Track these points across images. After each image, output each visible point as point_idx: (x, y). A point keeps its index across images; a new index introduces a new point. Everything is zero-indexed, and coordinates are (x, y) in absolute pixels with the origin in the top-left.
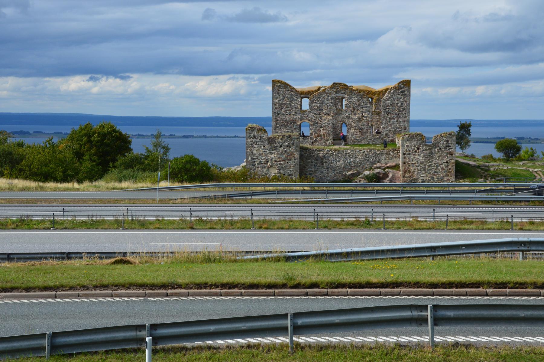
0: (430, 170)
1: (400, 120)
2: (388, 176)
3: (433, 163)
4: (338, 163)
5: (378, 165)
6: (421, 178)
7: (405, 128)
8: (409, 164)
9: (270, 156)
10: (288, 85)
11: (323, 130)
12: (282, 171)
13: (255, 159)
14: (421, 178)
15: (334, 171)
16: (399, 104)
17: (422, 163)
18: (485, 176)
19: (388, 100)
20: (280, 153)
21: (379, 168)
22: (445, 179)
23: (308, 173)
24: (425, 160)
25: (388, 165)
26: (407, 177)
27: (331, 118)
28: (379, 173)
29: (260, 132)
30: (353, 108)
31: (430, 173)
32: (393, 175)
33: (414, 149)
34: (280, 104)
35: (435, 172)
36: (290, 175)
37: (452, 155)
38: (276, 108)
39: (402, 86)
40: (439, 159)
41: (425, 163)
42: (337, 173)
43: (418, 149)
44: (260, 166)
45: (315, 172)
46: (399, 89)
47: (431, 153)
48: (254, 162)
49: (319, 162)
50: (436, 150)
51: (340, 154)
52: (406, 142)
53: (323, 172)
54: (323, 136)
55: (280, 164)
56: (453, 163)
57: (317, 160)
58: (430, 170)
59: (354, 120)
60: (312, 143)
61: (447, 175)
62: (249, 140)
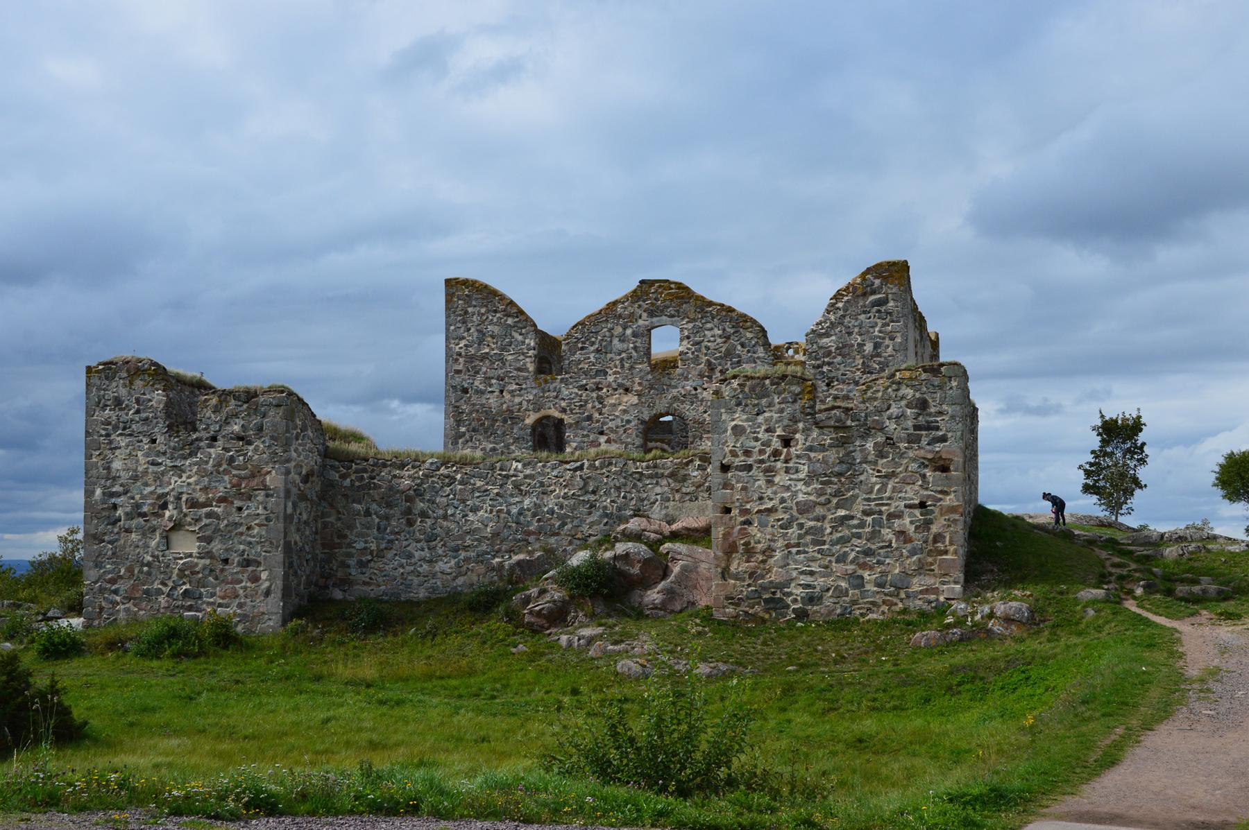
0: (843, 541)
2: (665, 573)
3: (859, 507)
4: (471, 517)
5: (634, 524)
6: (804, 579)
8: (745, 512)
9: (175, 483)
10: (494, 293)
11: (608, 441)
12: (217, 547)
13: (117, 495)
14: (804, 579)
15: (456, 550)
16: (869, 347)
17: (804, 508)
18: (1121, 578)
19: (827, 335)
20: (209, 467)
21: (637, 537)
22: (916, 584)
23: (352, 562)
24: (820, 493)
25: (674, 527)
26: (736, 577)
27: (635, 400)
28: (626, 557)
29: (138, 383)
30: (709, 363)
31: (842, 559)
32: (684, 569)
33: (767, 444)
34: (470, 359)
35: (868, 553)
36: (247, 563)
38: (458, 372)
39: (877, 282)
40: (884, 486)
41: (819, 511)
42: (467, 560)
43: (787, 442)
44: (134, 523)
45: (380, 554)
46: (865, 295)
47: (848, 461)
48: (115, 507)
49: (396, 511)
50: (870, 445)
51: (480, 477)
52: (731, 411)
53: (410, 556)
55: (209, 515)
56: (952, 509)
57: (389, 505)
58: (843, 541)
61: (922, 569)
62: (100, 416)
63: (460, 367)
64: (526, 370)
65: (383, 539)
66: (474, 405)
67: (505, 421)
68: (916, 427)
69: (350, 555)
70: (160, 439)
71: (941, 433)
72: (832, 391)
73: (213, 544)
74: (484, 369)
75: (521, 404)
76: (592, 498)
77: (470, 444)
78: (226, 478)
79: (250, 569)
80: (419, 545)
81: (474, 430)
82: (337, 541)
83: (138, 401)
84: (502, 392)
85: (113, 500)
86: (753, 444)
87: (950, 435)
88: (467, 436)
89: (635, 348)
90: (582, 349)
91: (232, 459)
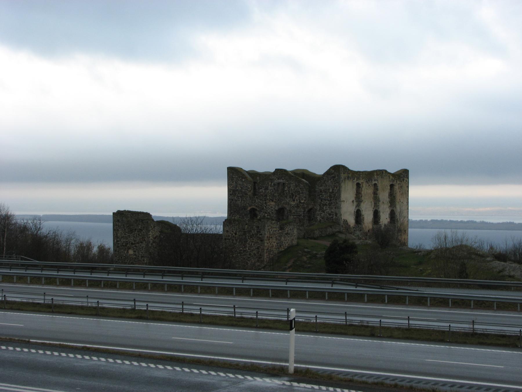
7: (336, 215)
16: (331, 190)
36: (142, 257)
37: (262, 241)
91: (139, 234)
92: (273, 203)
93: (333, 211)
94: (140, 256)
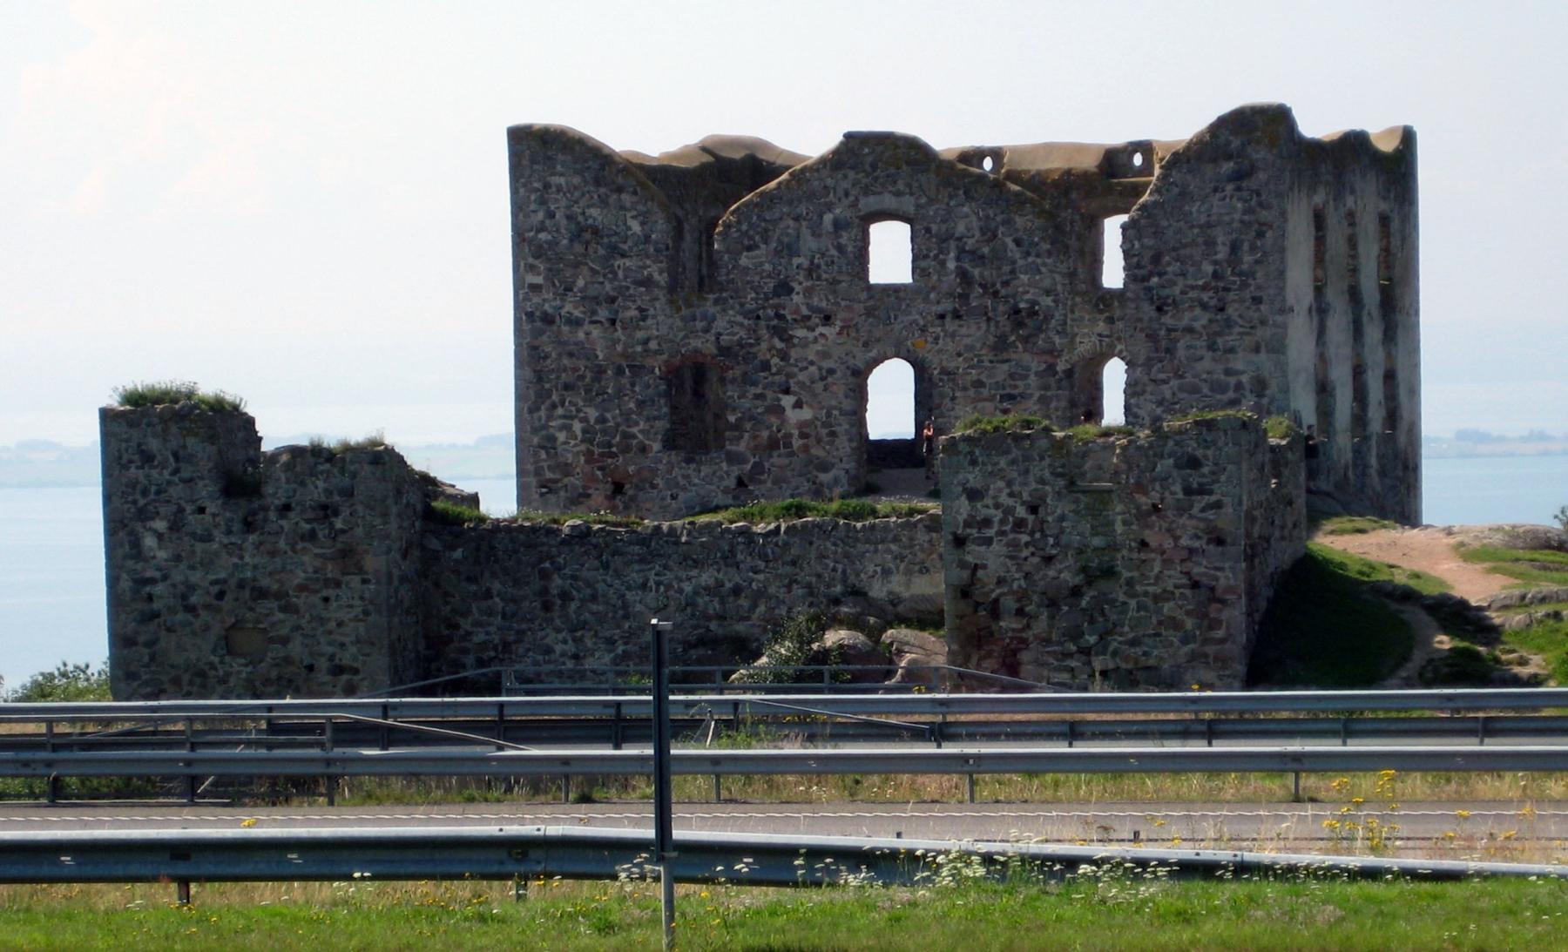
1: (1231, 339)
7: (1260, 386)
13: (152, 581)
36: (338, 670)
38: (535, 288)
39: (1236, 143)
48: (150, 598)
53: (549, 651)
54: (797, 443)
59: (970, 348)
60: (741, 483)
63: (539, 280)
64: (657, 285)
65: (510, 629)
66: (565, 343)
67: (619, 372)
68: (1188, 491)
69: (465, 651)
70: (211, 508)
71: (1213, 498)
72: (1167, 320)
73: (290, 646)
74: (581, 283)
75: (646, 342)
76: (788, 569)
77: (560, 411)
78: (306, 558)
79: (345, 677)
80: (560, 637)
81: (567, 387)
82: (446, 632)
83: (176, 455)
84: (613, 322)
85: (148, 589)
86: (992, 511)
87: (1225, 500)
88: (555, 397)
89: (840, 248)
90: (749, 249)
92: (831, 332)
93: (1240, 366)
94: (323, 664)
